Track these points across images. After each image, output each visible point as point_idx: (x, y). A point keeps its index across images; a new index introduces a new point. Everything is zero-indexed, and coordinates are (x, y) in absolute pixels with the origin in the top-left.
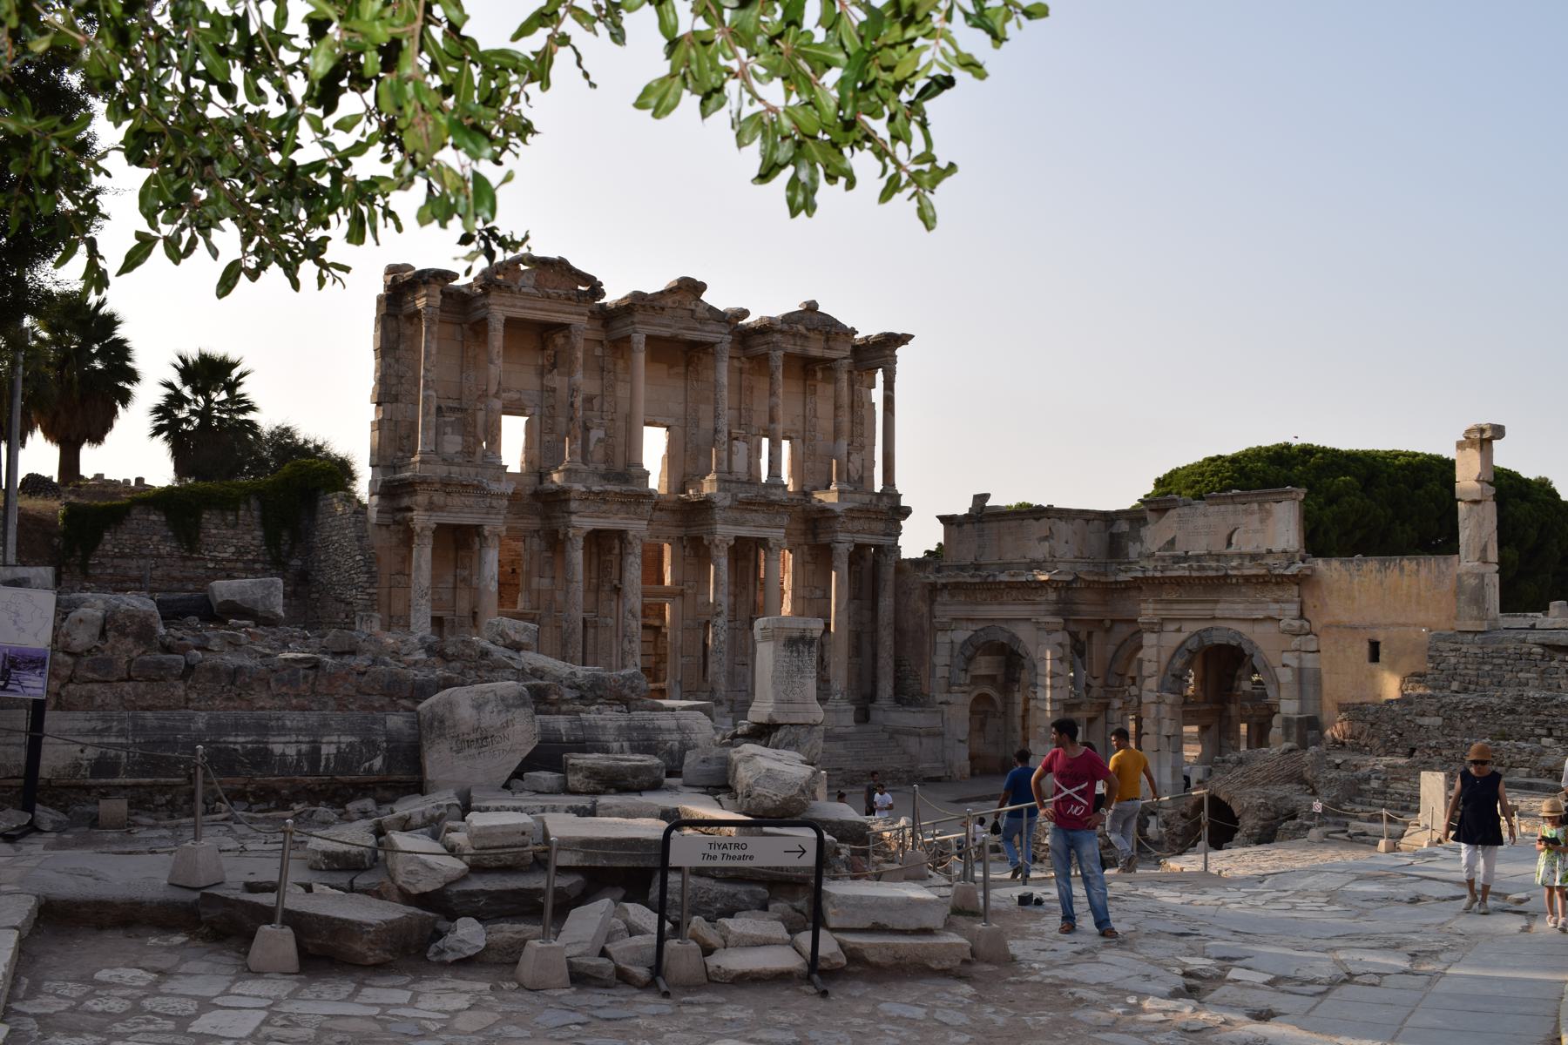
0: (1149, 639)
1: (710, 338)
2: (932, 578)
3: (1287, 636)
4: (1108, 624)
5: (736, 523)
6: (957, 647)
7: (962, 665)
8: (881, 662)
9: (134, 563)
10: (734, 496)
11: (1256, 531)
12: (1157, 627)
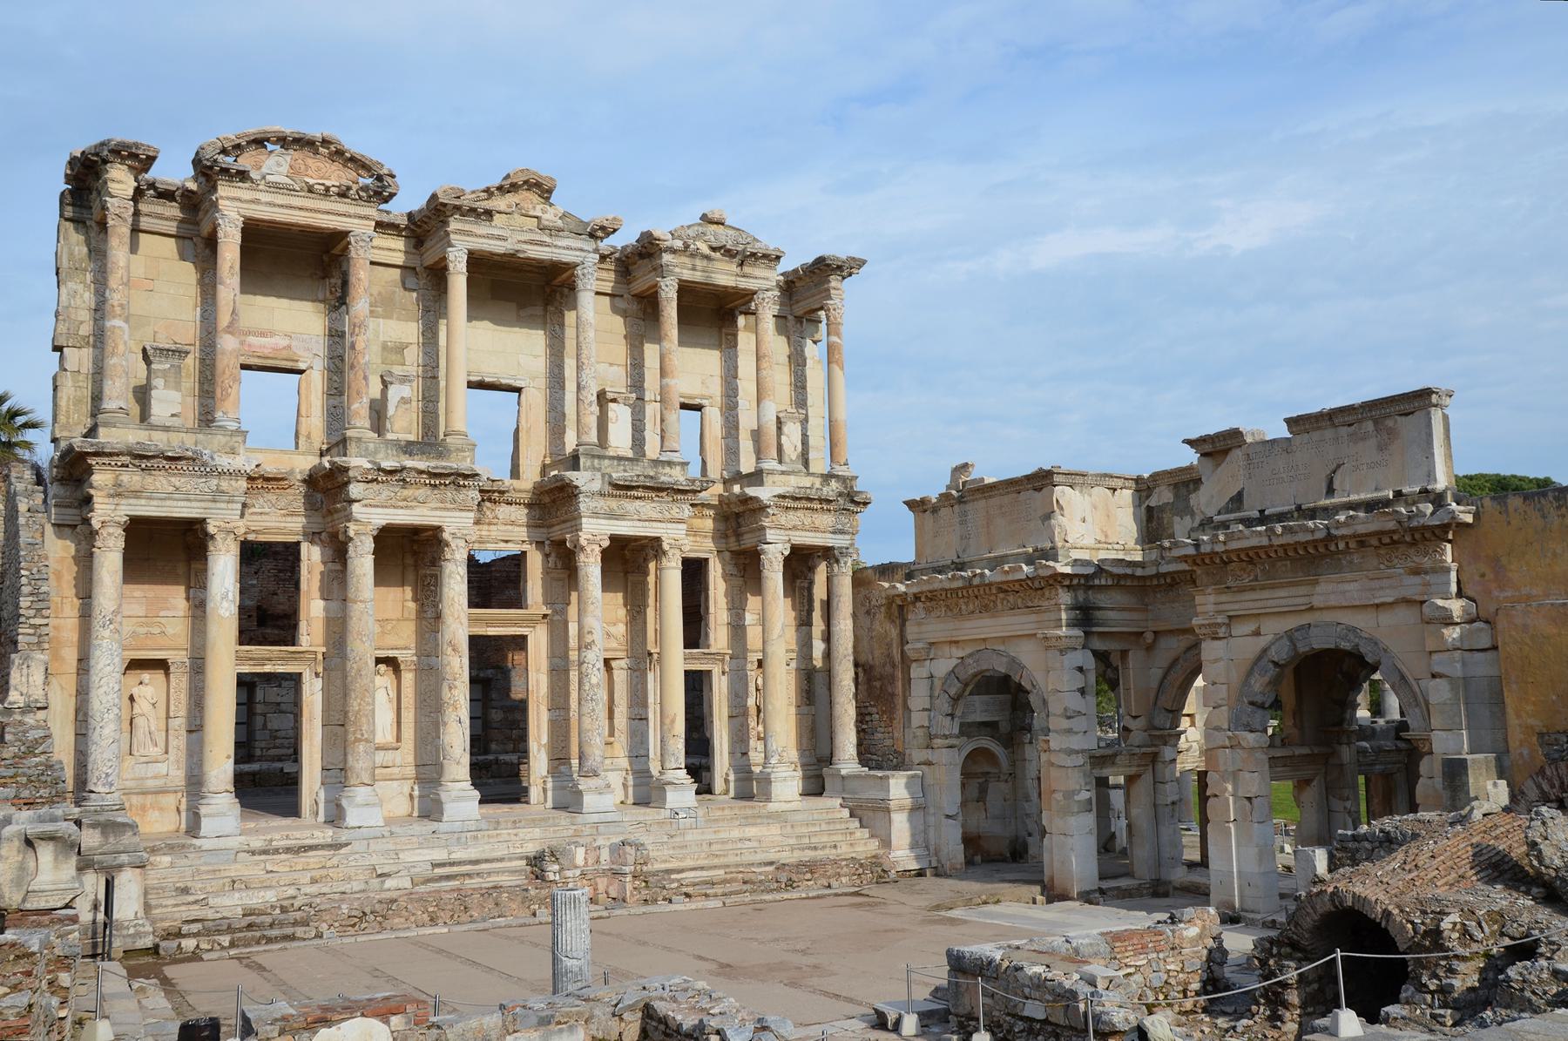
1: (567, 257)
2: (901, 588)
4: (1149, 637)
5: (612, 516)
6: (938, 683)
7: (947, 708)
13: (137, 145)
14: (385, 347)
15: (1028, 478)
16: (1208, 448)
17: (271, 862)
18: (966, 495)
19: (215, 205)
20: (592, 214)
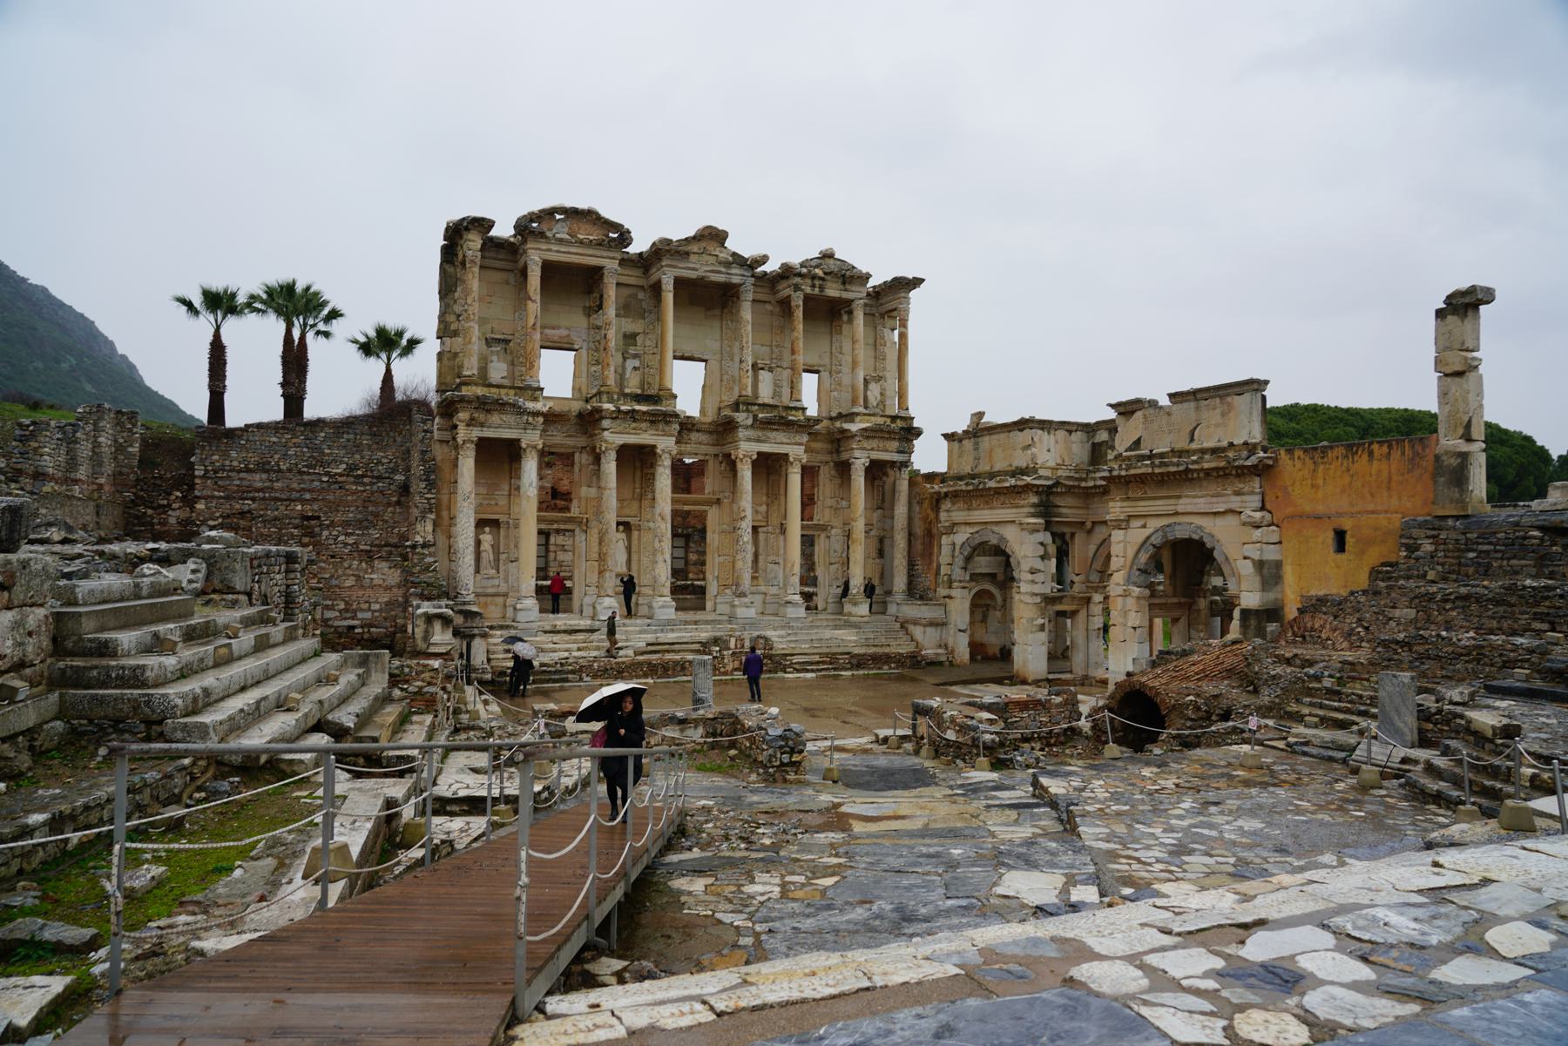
0: (1117, 535)
1: (736, 280)
3: (1247, 528)
4: (1089, 525)
5: (758, 441)
8: (896, 562)
9: (257, 477)
10: (755, 417)
11: (1217, 425)
12: (1123, 524)
13: (483, 219)
14: (625, 336)
15: (1015, 423)
16: (1122, 409)
17: (556, 638)
18: (979, 430)
19: (525, 252)
20: (747, 253)
